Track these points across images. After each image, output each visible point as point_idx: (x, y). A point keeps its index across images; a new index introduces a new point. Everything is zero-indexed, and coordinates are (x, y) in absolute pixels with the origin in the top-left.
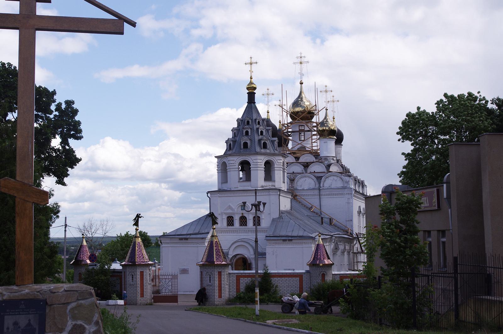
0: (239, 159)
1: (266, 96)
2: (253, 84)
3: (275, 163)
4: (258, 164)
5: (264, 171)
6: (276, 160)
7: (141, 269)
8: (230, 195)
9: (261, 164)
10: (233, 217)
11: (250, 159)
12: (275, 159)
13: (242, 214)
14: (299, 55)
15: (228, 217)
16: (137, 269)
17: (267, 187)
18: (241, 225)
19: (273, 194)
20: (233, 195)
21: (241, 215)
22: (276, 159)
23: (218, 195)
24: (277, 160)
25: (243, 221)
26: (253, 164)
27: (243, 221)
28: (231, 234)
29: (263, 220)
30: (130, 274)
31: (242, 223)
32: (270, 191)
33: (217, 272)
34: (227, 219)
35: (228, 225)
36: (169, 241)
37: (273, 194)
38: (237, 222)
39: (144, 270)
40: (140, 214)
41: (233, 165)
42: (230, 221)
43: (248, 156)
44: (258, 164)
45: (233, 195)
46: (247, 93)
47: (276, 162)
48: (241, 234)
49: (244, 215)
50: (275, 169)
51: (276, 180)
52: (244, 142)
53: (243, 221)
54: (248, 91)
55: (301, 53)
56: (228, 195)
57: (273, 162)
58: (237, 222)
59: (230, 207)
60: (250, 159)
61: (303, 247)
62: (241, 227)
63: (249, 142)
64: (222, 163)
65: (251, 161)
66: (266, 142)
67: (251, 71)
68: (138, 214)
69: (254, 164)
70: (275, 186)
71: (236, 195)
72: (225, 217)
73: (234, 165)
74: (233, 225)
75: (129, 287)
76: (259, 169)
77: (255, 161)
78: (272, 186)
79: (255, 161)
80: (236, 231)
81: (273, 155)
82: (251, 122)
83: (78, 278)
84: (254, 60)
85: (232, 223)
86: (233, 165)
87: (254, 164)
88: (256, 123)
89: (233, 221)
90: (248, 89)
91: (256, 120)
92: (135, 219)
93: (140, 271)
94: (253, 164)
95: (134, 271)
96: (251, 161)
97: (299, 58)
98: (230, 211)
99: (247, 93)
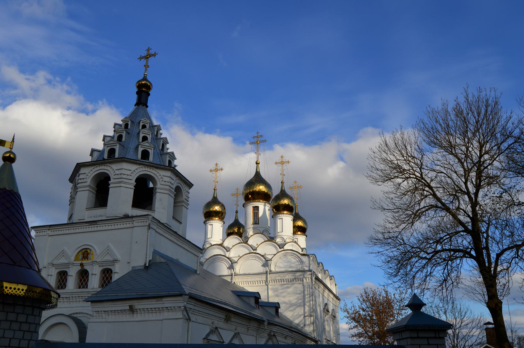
3: (158, 182)
11: (111, 170)
12: (158, 175)
14: (256, 135)
19: (140, 224)
24: (163, 177)
31: (82, 284)
37: (140, 224)
41: (82, 181)
48: (75, 304)
50: (158, 190)
59: (63, 254)
60: (111, 170)
61: (162, 320)
67: (147, 66)
77: (117, 172)
84: (152, 52)
86: (82, 181)
87: (116, 177)
96: (112, 172)
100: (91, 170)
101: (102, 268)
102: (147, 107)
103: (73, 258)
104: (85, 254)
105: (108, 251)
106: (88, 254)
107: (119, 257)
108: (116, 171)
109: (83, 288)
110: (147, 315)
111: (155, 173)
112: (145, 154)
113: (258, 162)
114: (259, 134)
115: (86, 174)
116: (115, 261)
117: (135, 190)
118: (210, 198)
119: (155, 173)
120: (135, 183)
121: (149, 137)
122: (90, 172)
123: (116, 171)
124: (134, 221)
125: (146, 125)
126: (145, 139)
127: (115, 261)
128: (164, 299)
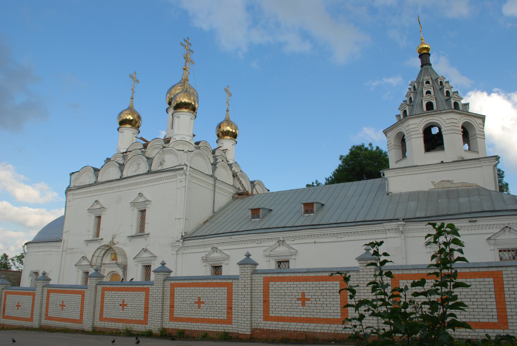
0: (425, 120)
5: (462, 135)
6: (477, 125)
9: (457, 125)
11: (441, 120)
12: (475, 123)
22: (477, 123)
32: (481, 160)
41: (414, 130)
47: (478, 127)
60: (441, 120)
63: (434, 102)
64: (397, 133)
65: (443, 121)
73: (416, 129)
82: (432, 82)
91: (436, 80)
94: (445, 125)
96: (443, 121)
100: (421, 121)
102: (430, 65)
108: (446, 121)
112: (430, 106)
115: (417, 124)
117: (463, 135)
120: (462, 130)
121: (432, 91)
122: (421, 122)
123: (446, 121)
124: (481, 161)
125: (429, 80)
126: (428, 92)
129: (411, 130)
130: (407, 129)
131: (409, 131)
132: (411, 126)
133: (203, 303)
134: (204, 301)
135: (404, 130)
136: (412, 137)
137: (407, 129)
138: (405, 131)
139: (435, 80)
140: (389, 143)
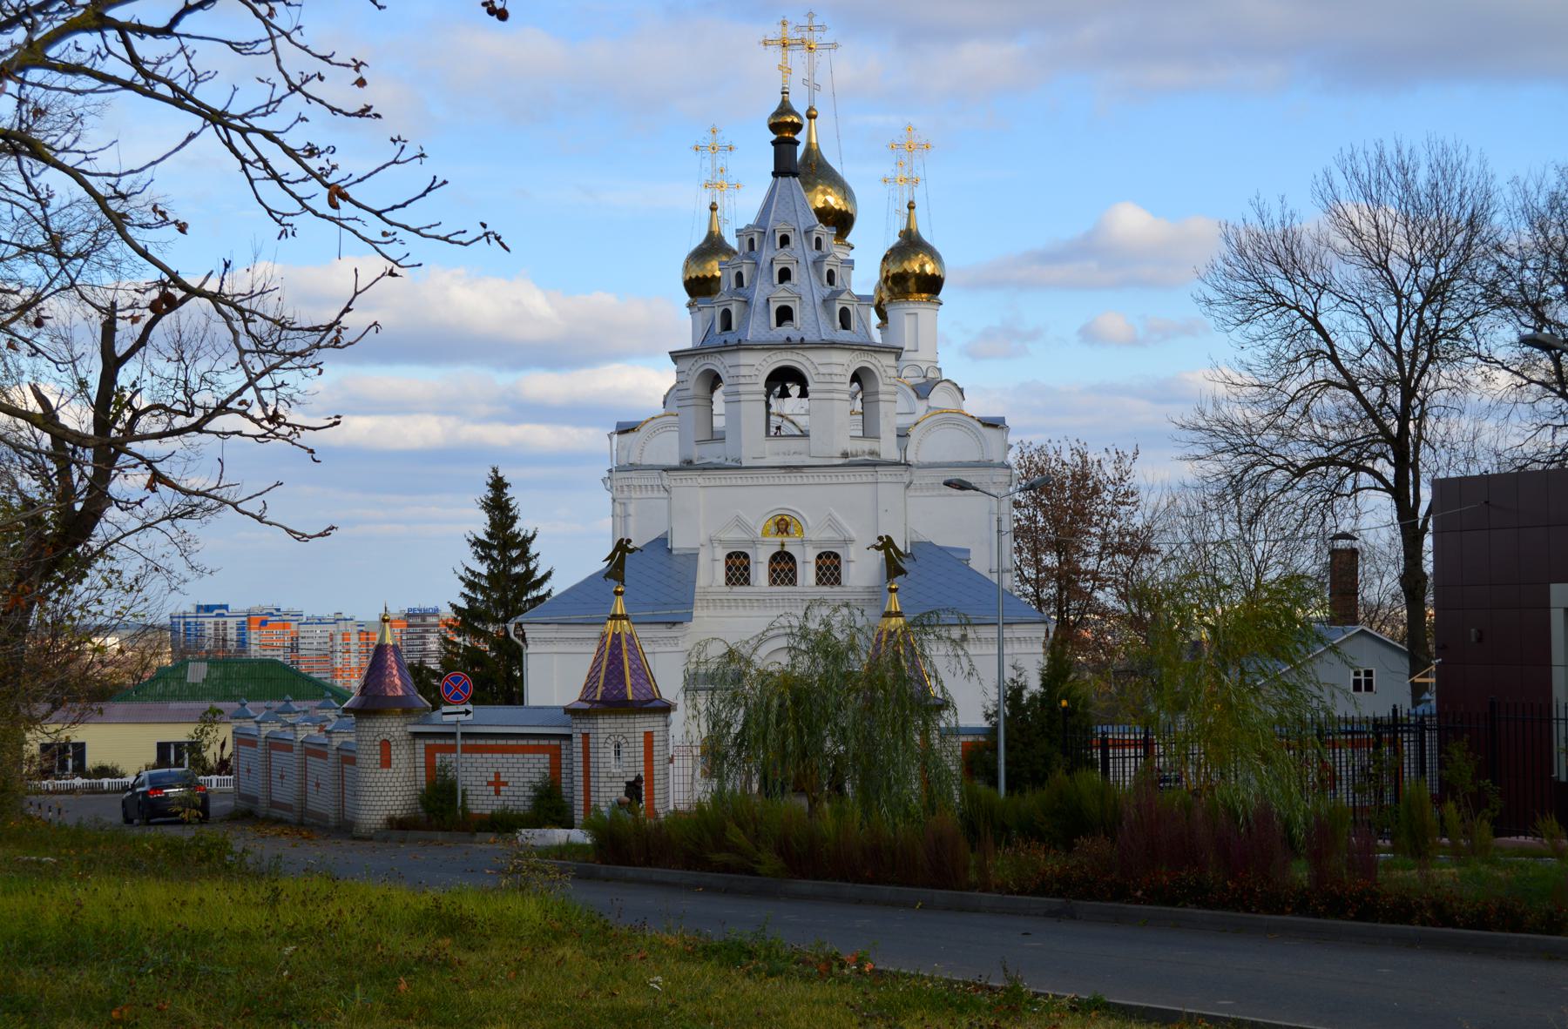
0: (775, 358)
1: (708, 154)
2: (791, 112)
3: (880, 380)
4: (836, 379)
6: (882, 370)
7: (647, 724)
8: (740, 482)
10: (746, 556)
12: (879, 365)
13: (783, 545)
14: (806, 22)
15: (729, 556)
16: (637, 725)
17: (857, 456)
18: (773, 582)
19: (890, 479)
20: (750, 482)
21: (777, 549)
23: (700, 480)
25: (783, 568)
26: (816, 378)
27: (782, 570)
28: (741, 611)
29: (852, 565)
30: (608, 741)
32: (878, 469)
33: (580, 735)
34: (727, 563)
35: (729, 581)
36: (554, 635)
37: (890, 479)
38: (760, 572)
39: (656, 729)
40: (629, 541)
41: (748, 380)
42: (738, 568)
43: (718, 356)
44: (836, 379)
45: (750, 482)
46: (773, 143)
49: (786, 549)
50: (881, 397)
51: (882, 435)
52: (779, 304)
53: (783, 568)
54: (774, 137)
55: (811, 15)
56: (734, 482)
57: (875, 377)
58: (760, 572)
59: (739, 523)
60: (807, 364)
62: (775, 588)
65: (810, 367)
66: (848, 307)
68: (622, 540)
69: (822, 379)
70: (878, 455)
71: (761, 482)
72: (721, 555)
74: (747, 582)
75: (607, 784)
76: (836, 396)
78: (872, 453)
79: (822, 370)
80: (761, 602)
81: (875, 351)
83: (378, 757)
85: (742, 575)
86: (748, 380)
87: (822, 379)
88: (810, 244)
89: (747, 569)
90: (774, 127)
92: (611, 557)
93: (643, 730)
94: (816, 378)
95: (622, 730)
96: (810, 367)
97: (804, 29)
98: (735, 535)
99: (773, 143)
101: (819, 551)
103: (759, 532)
104: (783, 526)
105: (832, 523)
106: (787, 525)
107: (854, 535)
108: (819, 367)
109: (783, 582)
110: (984, 647)
111: (873, 361)
113: (814, 113)
114: (816, 22)
116: (847, 542)
118: (698, 239)
119: (873, 361)
123: (819, 367)
127: (847, 542)
128: (1014, 627)
129: (742, 380)
130: (732, 371)
131: (735, 381)
132: (744, 371)
133: (505, 784)
134: (506, 779)
135: (724, 372)
136: (743, 397)
137: (732, 371)
138: (726, 375)
139: (806, 232)
140: (681, 386)
